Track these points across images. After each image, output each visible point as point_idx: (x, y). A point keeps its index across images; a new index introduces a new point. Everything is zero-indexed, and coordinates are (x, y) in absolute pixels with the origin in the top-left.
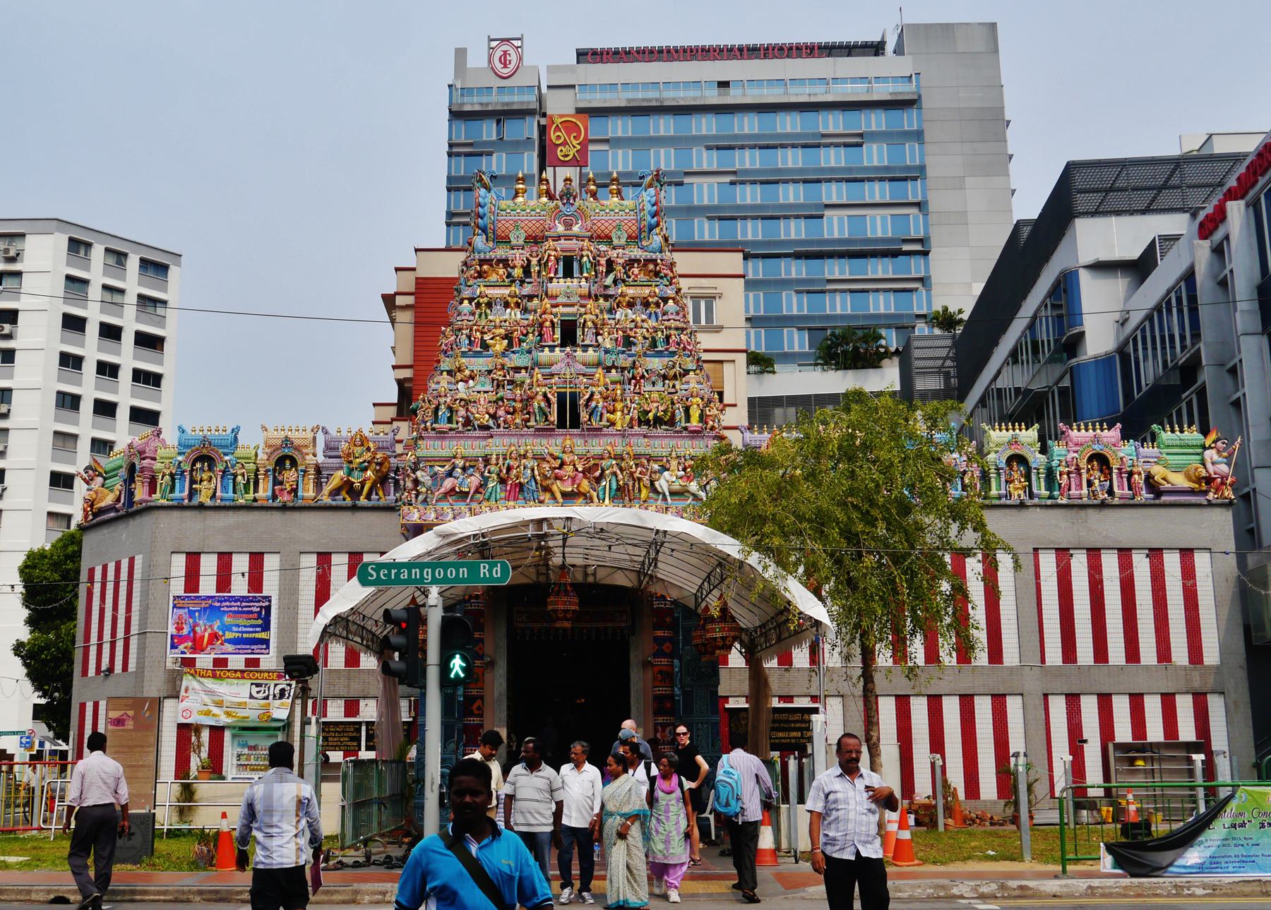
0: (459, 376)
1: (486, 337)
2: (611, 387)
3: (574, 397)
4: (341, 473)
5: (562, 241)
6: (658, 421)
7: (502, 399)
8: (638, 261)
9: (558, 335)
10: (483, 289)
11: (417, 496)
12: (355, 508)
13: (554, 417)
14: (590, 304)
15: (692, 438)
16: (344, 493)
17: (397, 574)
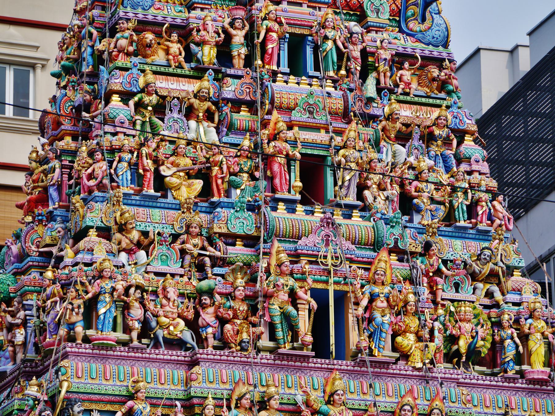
6: (474, 356)
7: (210, 292)
8: (411, 58)
10: (150, 77)
14: (353, 129)
15: (531, 392)
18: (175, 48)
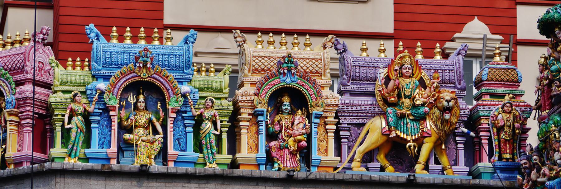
16: (381, 159)
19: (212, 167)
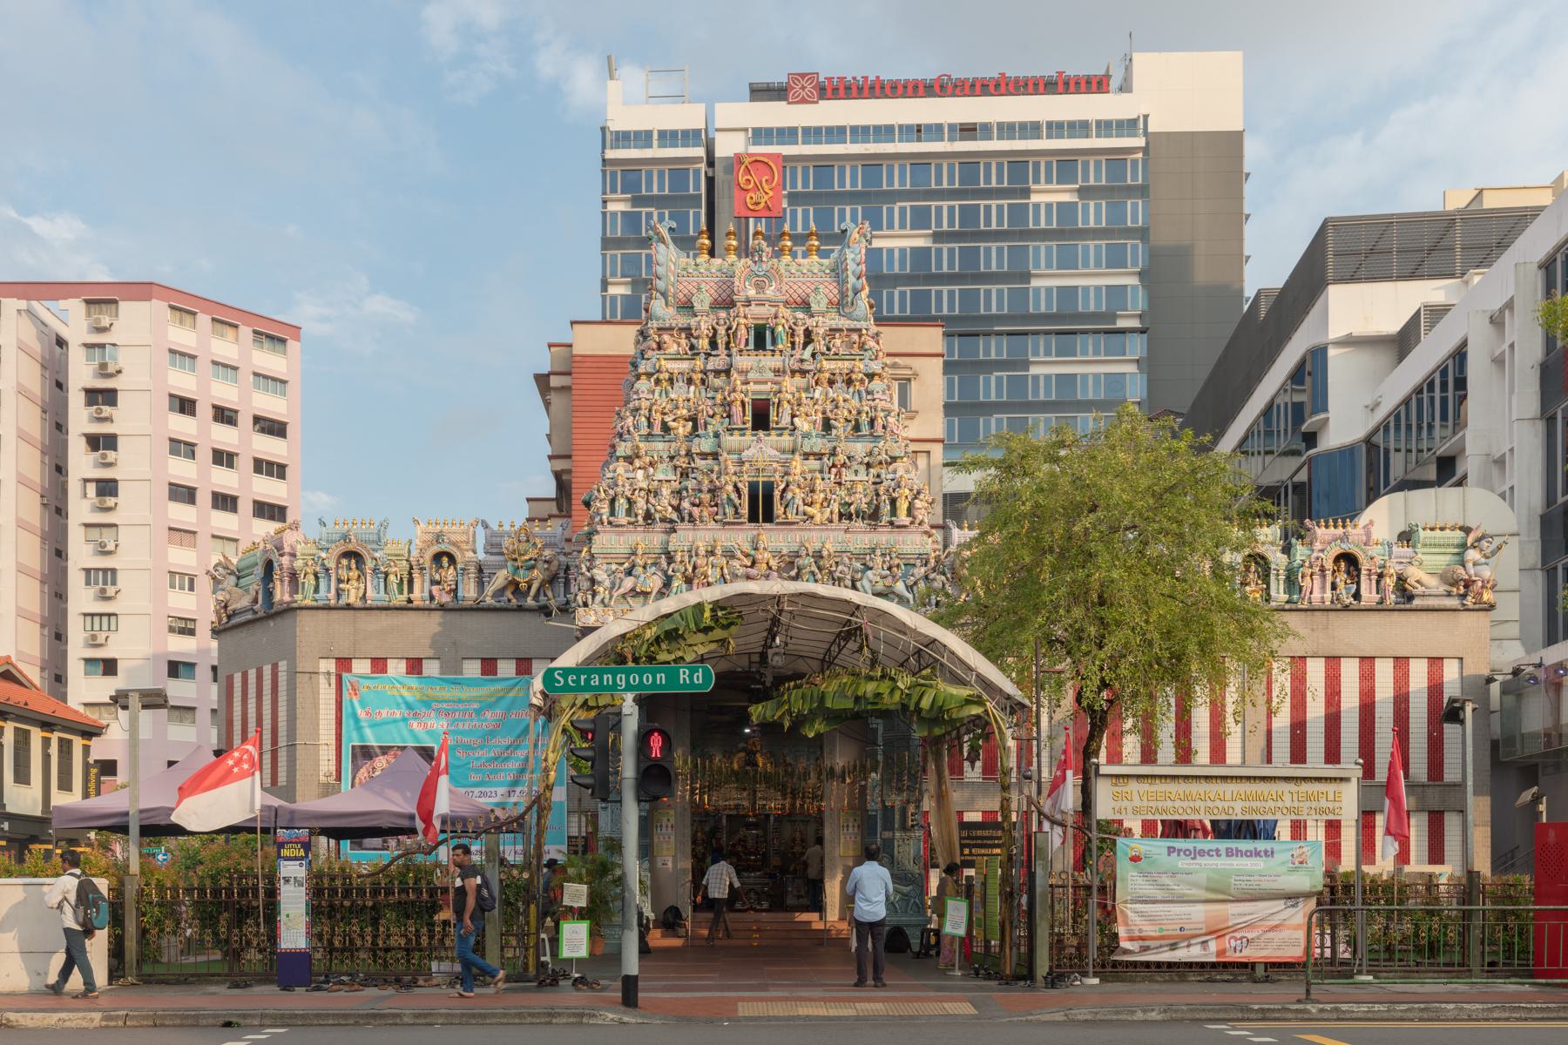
0: (637, 463)
1: (667, 419)
2: (809, 476)
3: (769, 488)
4: (505, 572)
5: (753, 307)
9: (749, 418)
11: (594, 596)
12: (520, 609)
13: (745, 511)
17: (587, 681)
18: (684, 342)
19: (395, 603)
